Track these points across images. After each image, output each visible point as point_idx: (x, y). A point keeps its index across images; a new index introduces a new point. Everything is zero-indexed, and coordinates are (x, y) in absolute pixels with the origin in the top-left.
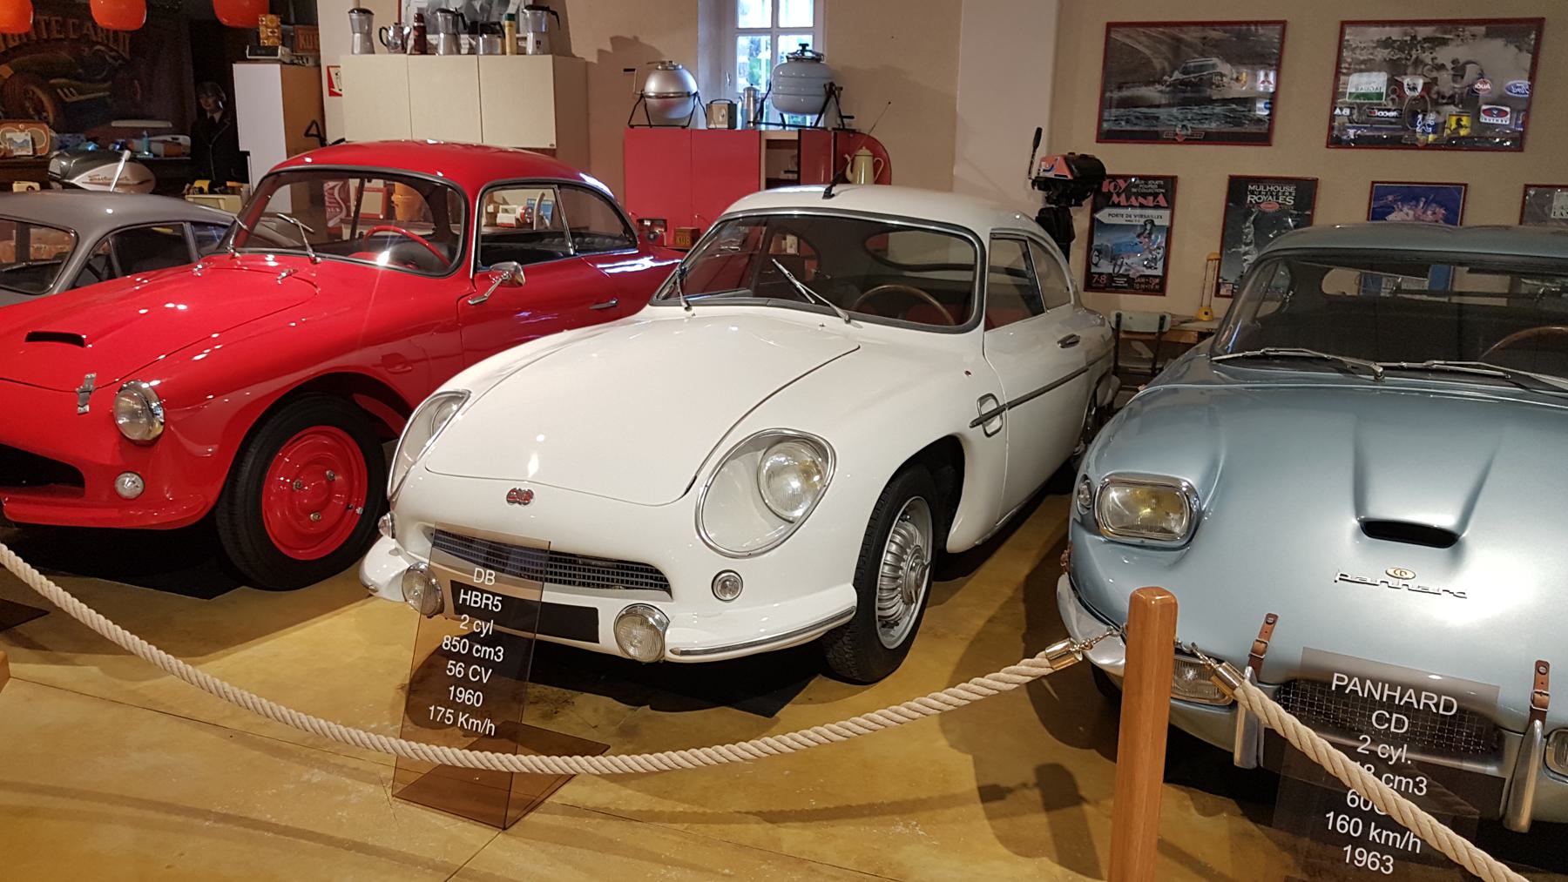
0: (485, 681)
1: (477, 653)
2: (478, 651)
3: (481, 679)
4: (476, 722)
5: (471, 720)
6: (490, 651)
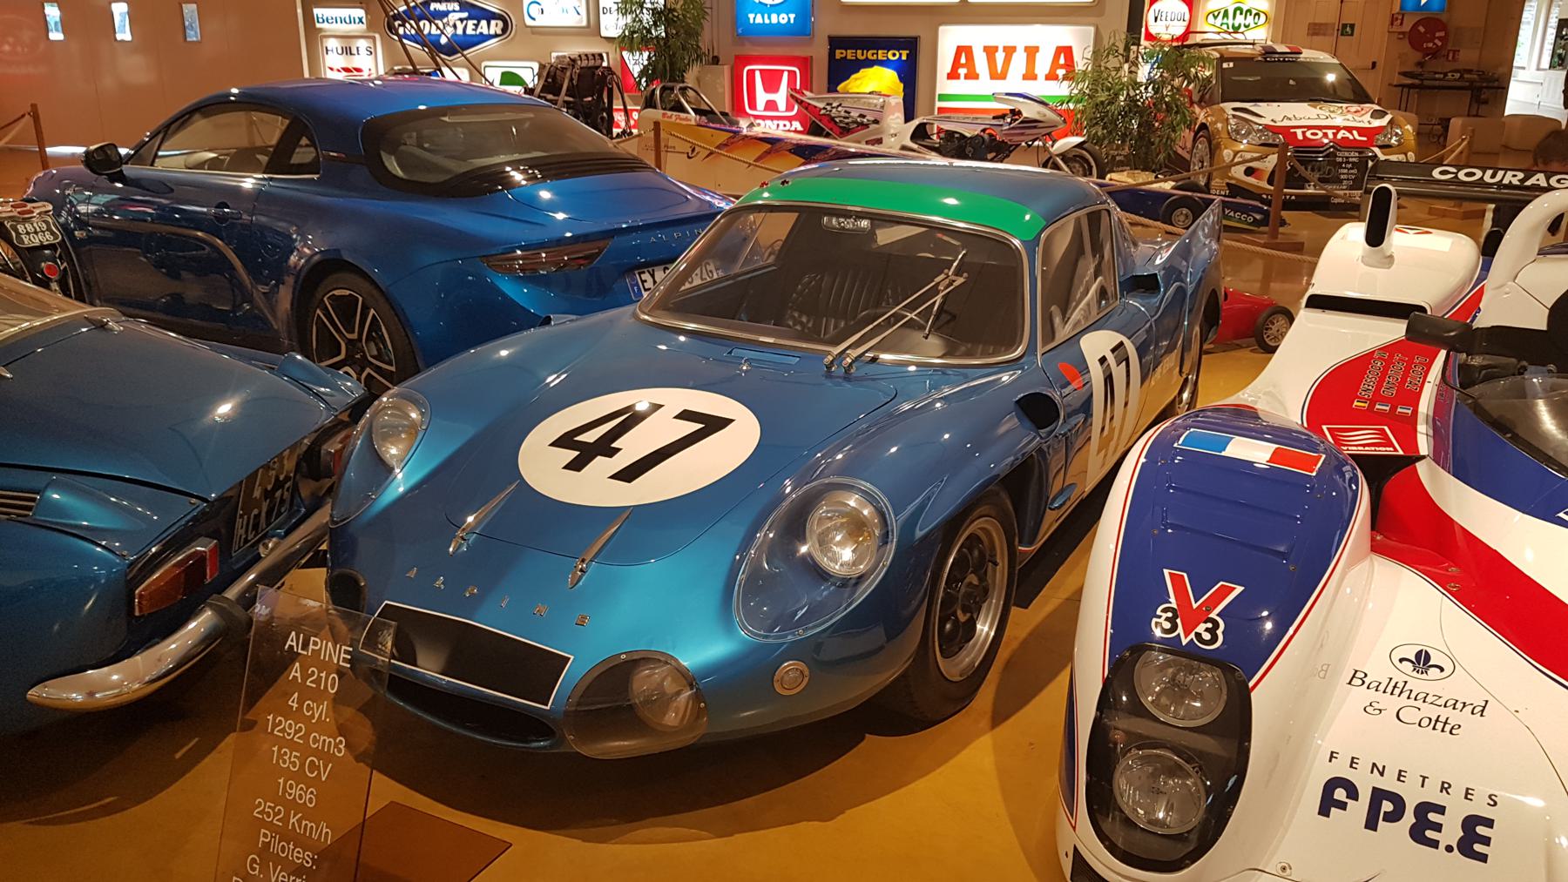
0: (324, 779)
1: (314, 744)
2: (315, 741)
3: (319, 773)
4: (309, 825)
5: (304, 822)
6: (330, 742)
